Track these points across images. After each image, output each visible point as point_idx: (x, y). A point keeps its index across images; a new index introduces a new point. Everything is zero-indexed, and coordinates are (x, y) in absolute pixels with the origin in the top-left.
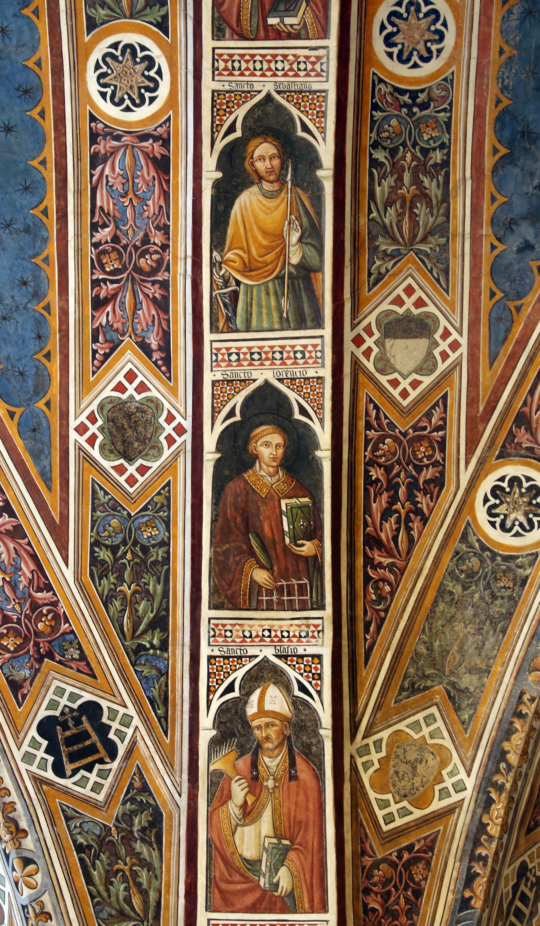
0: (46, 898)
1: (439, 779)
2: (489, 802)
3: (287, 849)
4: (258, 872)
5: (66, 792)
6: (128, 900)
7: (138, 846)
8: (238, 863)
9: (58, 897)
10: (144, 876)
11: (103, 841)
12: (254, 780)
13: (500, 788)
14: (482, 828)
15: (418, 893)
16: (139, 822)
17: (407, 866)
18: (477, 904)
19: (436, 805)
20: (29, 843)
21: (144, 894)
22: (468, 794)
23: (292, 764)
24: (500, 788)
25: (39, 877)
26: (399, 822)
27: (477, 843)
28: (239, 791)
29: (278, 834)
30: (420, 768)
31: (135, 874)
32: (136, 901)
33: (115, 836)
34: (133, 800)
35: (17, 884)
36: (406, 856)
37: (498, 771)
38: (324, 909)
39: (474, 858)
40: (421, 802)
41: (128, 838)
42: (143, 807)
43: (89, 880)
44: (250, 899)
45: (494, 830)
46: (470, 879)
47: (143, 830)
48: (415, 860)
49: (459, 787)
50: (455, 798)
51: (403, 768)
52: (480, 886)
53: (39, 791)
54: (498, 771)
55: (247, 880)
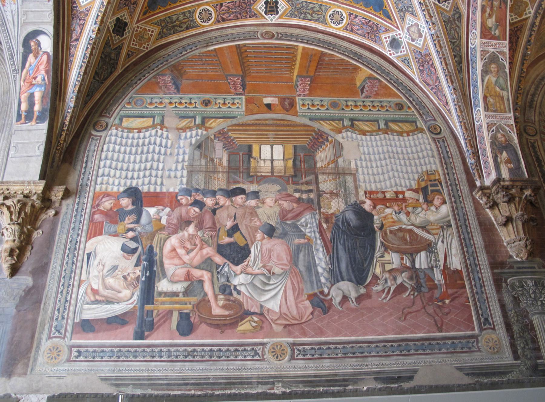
0: (438, 33)
1: (525, 11)
2: (537, 17)
3: (498, 25)
4: (491, 30)
5: (440, 7)
6: (455, 35)
7: (457, 22)
8: (487, 28)
9: (440, 33)
10: (458, 29)
11: (449, 19)
12: (492, 8)
13: (540, 14)
14: (534, 23)
15: (518, 38)
16: (457, 16)
17: (516, 31)
18: (532, 41)
19: (524, 17)
20: (433, 19)
21: (458, 34)
22: (532, 14)
23: (500, 4)
24: (540, 14)
25: (436, 28)
26: (515, 21)
27: (533, 27)
28: (488, 10)
29: (496, 21)
30: (521, 8)
31: (456, 29)
32: (456, 35)
33: (452, 19)
34: (455, 11)
35: (430, 29)
36: (516, 29)
37: (539, 9)
38: (506, 40)
39: (532, 30)
40: (520, 16)
41: (454, 20)
42: (457, 12)
43: (447, 30)
44: (490, 36)
45: (537, 24)
46: (531, 35)
47: (457, 18)
48: (518, 30)
49: (530, 13)
50: (529, 15)
51: (517, 7)
52: (533, 37)
53: (435, 7)
54: (539, 9)
55: (489, 32)
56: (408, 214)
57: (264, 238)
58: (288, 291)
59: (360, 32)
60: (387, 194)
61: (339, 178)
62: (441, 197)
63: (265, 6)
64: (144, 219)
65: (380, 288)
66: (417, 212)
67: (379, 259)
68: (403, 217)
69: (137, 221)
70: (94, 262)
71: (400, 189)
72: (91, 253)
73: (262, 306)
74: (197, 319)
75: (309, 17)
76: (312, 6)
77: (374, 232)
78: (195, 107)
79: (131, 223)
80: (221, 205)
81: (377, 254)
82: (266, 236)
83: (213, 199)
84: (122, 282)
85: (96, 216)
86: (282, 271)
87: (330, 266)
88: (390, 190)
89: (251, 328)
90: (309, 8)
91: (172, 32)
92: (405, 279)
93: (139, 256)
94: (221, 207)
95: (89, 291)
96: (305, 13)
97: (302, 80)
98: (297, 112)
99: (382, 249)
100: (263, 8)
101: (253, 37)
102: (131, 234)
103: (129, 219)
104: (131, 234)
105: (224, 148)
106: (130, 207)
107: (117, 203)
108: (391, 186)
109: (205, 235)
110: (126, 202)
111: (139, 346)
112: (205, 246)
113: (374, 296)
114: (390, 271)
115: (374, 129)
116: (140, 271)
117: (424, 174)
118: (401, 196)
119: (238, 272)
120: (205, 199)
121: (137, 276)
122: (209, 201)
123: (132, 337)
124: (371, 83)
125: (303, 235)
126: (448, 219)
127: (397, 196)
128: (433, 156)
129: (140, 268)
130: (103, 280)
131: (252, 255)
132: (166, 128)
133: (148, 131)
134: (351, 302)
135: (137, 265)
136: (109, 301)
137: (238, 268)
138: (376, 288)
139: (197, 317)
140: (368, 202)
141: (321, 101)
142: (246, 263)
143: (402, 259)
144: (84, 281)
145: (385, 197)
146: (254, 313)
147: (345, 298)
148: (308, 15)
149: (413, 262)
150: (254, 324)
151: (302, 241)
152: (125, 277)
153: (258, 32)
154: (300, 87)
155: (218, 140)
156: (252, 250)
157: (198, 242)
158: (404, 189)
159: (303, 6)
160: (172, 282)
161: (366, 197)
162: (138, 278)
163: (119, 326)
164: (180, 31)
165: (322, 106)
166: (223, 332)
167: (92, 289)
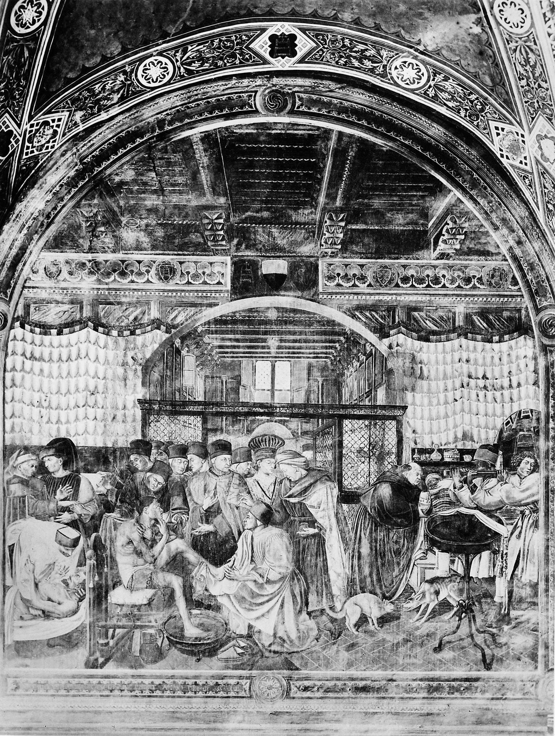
56: (473, 489)
57: (256, 527)
58: (286, 605)
59: (450, 104)
60: (446, 454)
61: (376, 424)
62: (532, 461)
63: (269, 43)
64: (85, 493)
65: (413, 605)
66: (488, 486)
67: (419, 561)
68: (465, 494)
69: (75, 495)
70: (19, 560)
71: (469, 445)
72: (13, 545)
73: (250, 627)
74: (166, 642)
75: (356, 64)
76: (361, 47)
77: (417, 519)
78: (148, 281)
79: (64, 500)
80: (194, 470)
81: (417, 554)
82: (259, 523)
83: (183, 460)
84: (63, 590)
85: (13, 487)
86: (280, 576)
87: (347, 570)
88: (452, 446)
89: (236, 655)
90: (355, 49)
91: (96, 110)
92: (452, 594)
93: (83, 551)
94: (195, 474)
95: (19, 601)
96: (349, 57)
97: (331, 218)
98: (316, 294)
99: (425, 546)
100: (267, 46)
101: (247, 108)
102: (66, 517)
103: (62, 492)
104: (66, 517)
105: (197, 366)
106: (61, 473)
107: (42, 469)
108: (456, 439)
109: (173, 521)
110: (54, 464)
111: (92, 677)
112: (173, 537)
113: (403, 618)
114: (432, 581)
115: (447, 328)
116: (85, 573)
117: (513, 417)
118: (467, 458)
119: (221, 576)
120: (170, 460)
121: (81, 581)
122: (177, 465)
123: (83, 664)
124: (455, 222)
125: (312, 523)
126: (535, 498)
127: (462, 458)
128: (536, 383)
129: (86, 568)
130: (36, 585)
131: (239, 552)
132: (103, 326)
133: (74, 331)
134: (371, 624)
135: (81, 564)
136: (46, 615)
137: (221, 571)
138: (408, 605)
139: (166, 639)
140: (416, 468)
141: (362, 266)
142: (230, 564)
143: (452, 562)
144: (9, 587)
145: (443, 458)
146: (241, 636)
147: (363, 619)
148: (354, 61)
149: (468, 566)
150: (240, 651)
151: (312, 531)
152: (65, 582)
153: (256, 92)
154: (328, 235)
155: (188, 352)
156: (239, 544)
157: (162, 529)
158: (476, 446)
159: (344, 46)
160: (131, 589)
161: (413, 459)
162: (83, 584)
163: (65, 650)
164: (111, 106)
165: (363, 278)
166: (199, 660)
167: (22, 599)
